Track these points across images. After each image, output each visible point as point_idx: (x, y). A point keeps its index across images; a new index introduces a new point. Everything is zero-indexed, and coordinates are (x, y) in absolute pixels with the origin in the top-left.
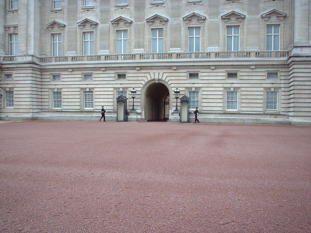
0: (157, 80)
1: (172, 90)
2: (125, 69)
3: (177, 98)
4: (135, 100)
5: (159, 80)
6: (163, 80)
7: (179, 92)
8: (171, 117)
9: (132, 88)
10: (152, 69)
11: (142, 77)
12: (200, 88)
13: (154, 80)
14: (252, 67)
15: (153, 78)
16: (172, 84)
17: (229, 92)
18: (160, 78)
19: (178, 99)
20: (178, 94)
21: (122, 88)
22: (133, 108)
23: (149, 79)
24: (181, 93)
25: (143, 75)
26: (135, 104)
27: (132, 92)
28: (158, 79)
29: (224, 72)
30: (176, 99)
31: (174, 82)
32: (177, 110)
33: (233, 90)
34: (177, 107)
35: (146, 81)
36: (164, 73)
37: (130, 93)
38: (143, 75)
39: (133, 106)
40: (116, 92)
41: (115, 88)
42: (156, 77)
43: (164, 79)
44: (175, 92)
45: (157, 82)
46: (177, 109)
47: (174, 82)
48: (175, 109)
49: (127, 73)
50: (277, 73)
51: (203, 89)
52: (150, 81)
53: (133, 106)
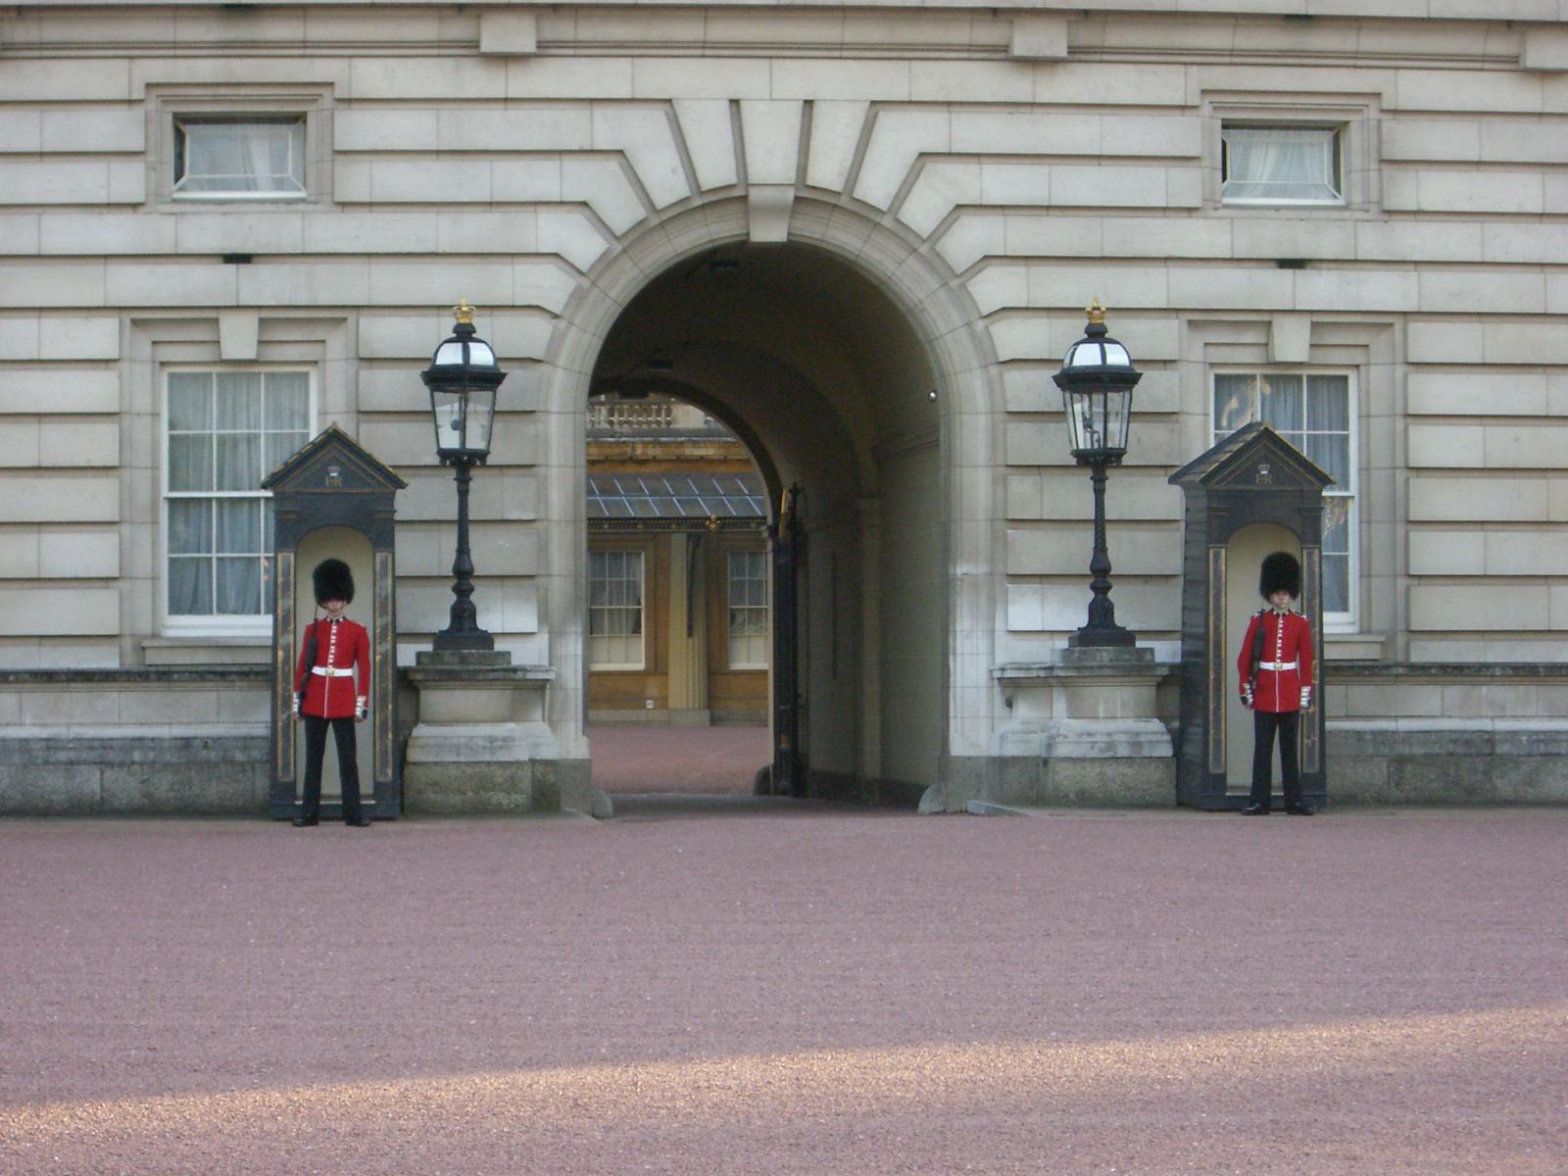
0: (771, 210)
1: (993, 343)
2: (306, 48)
3: (1099, 462)
4: (488, 494)
5: (808, 199)
6: (864, 215)
7: (1123, 380)
8: (976, 726)
9: (447, 326)
10: (706, 49)
11: (549, 166)
12: (1380, 321)
13: (734, 199)
14: (1028, 40)
15: (716, 171)
16: (993, 272)
17: (195, 376)
18: (827, 172)
19: (1115, 482)
20: (1115, 399)
21: (250, 321)
22: (463, 613)
23: (667, 185)
24: (1151, 390)
25: (570, 128)
26: (486, 553)
27: (441, 379)
28: (790, 194)
29: (130, 102)
30: (1084, 480)
31: (1026, 235)
32: (1101, 628)
33: (251, 355)
34: (1111, 595)
35: (623, 212)
36: (887, 120)
37: (405, 388)
38: (570, 128)
39: (463, 577)
40: (143, 371)
41: (140, 318)
42: (772, 162)
43: (876, 188)
44: (1076, 381)
45: (770, 232)
46: (1100, 611)
47: (1026, 235)
48: (1079, 619)
49: (326, 102)
50: (1337, 131)
51: (1431, 341)
52: (683, 212)
53: (463, 577)
